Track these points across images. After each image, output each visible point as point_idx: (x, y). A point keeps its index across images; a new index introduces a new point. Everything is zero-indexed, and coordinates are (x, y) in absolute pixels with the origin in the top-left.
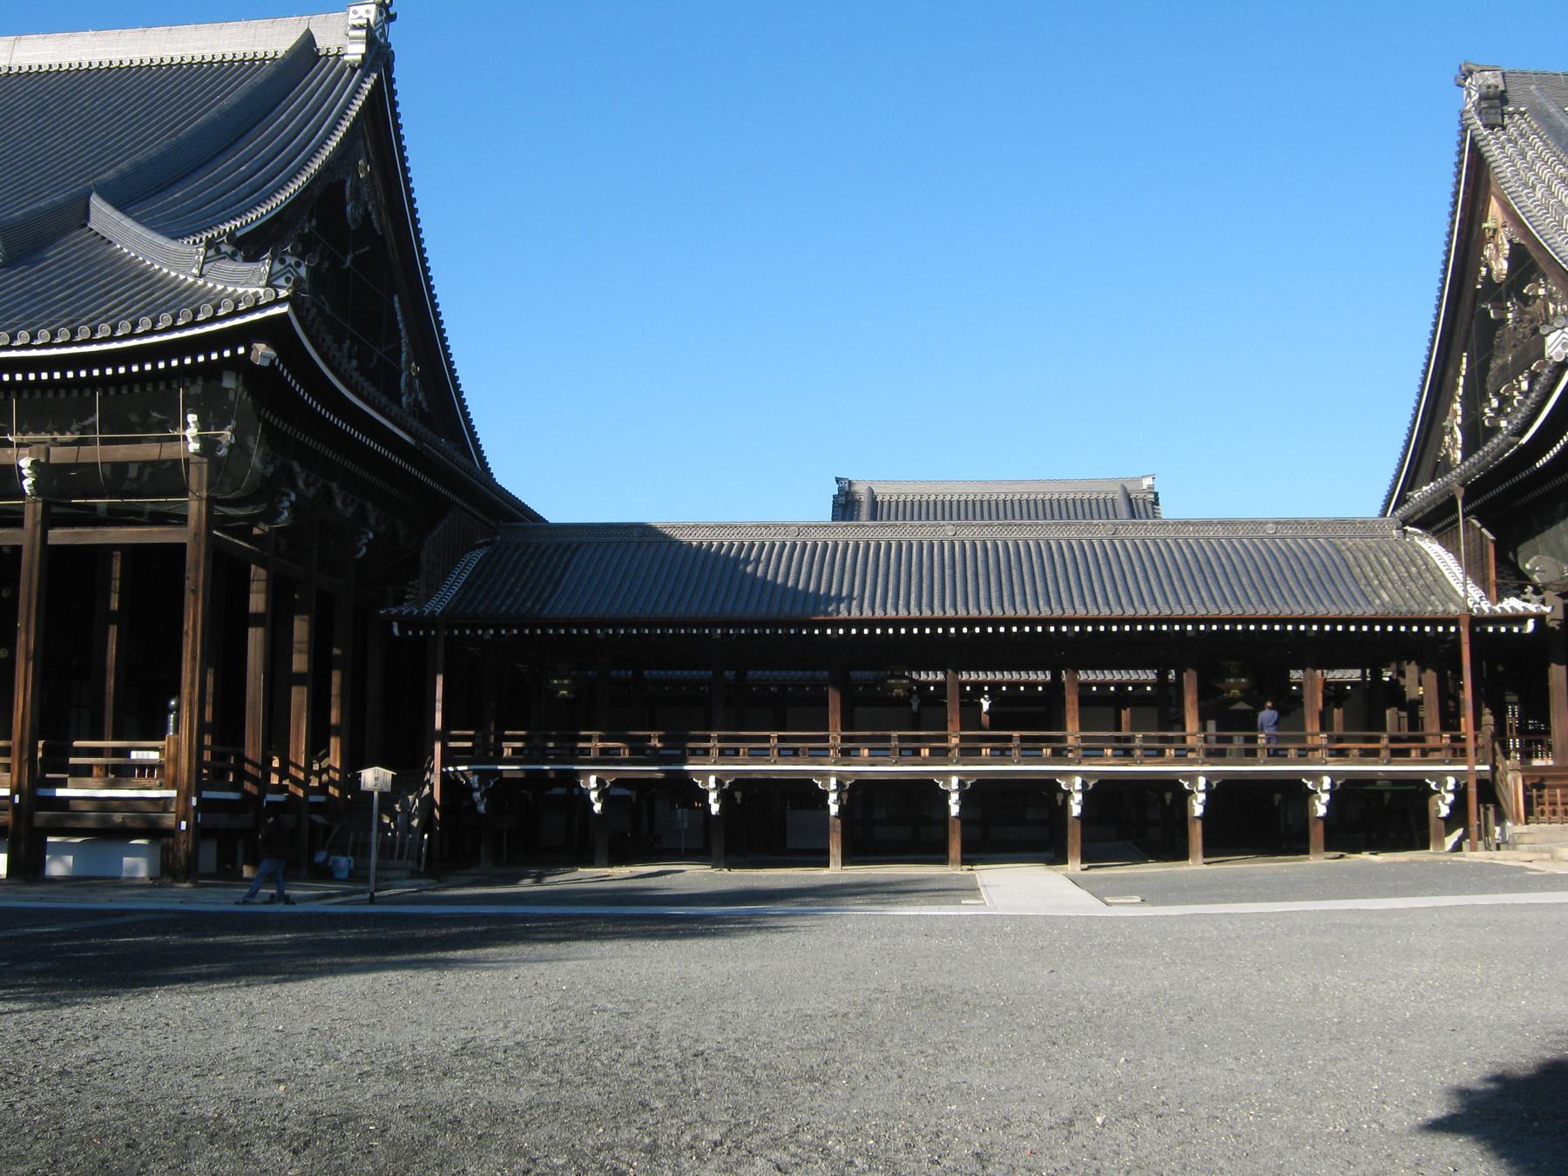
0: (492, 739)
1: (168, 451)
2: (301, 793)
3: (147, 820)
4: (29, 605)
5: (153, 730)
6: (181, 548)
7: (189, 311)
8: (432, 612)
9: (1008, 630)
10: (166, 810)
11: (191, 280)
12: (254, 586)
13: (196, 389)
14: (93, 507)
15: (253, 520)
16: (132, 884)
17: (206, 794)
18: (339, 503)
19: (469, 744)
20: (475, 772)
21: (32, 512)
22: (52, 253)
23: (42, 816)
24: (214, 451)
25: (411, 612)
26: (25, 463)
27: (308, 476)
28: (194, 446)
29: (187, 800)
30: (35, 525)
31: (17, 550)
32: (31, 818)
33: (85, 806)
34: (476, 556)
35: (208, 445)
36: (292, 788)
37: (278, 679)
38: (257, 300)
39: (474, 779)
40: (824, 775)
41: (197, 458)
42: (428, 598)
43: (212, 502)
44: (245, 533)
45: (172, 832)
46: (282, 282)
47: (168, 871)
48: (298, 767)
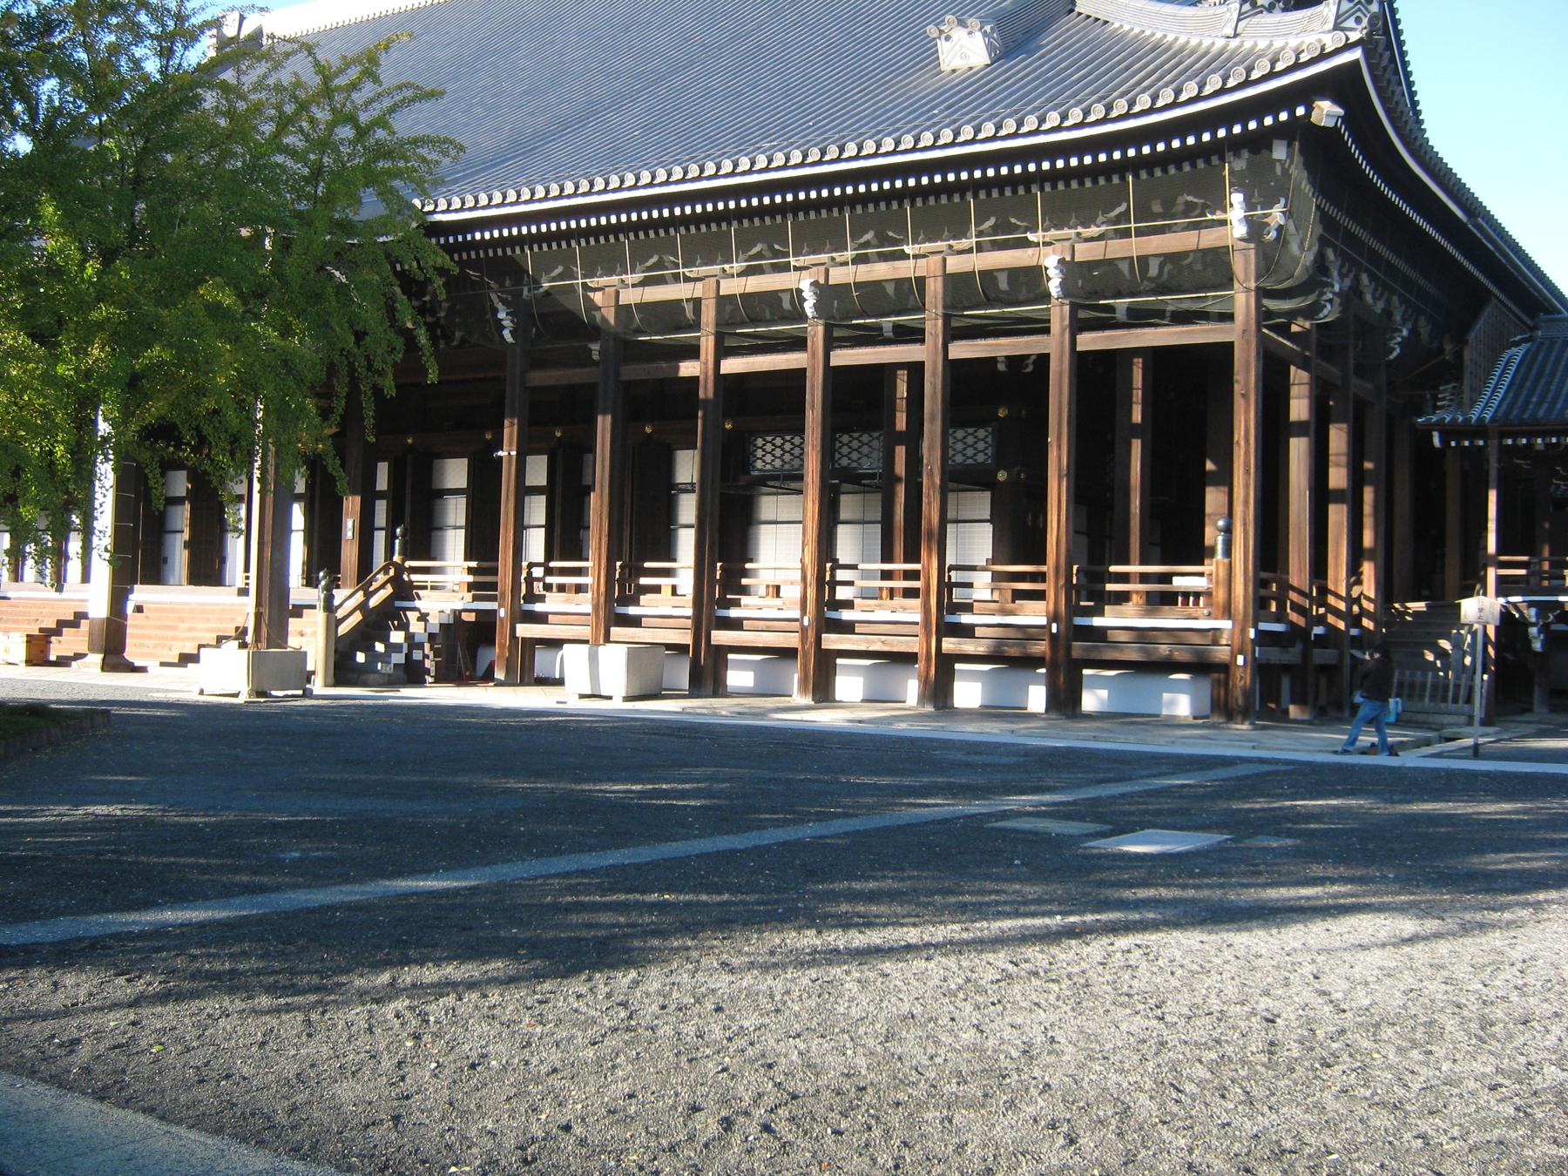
0: (1546, 566)
1: (1209, 238)
2: (1341, 625)
3: (1198, 653)
4: (1060, 415)
5: (1196, 553)
6: (1228, 347)
7: (1241, 70)
8: (1480, 420)
10: (1216, 643)
11: (1220, 43)
12: (1294, 391)
13: (1240, 164)
14: (1111, 309)
15: (1292, 315)
16: (1173, 723)
17: (1263, 626)
18: (1369, 298)
19: (1523, 572)
20: (1531, 604)
21: (1059, 315)
22: (1048, 40)
23: (1078, 648)
24: (1262, 236)
25: (1454, 420)
26: (1050, 261)
27: (1341, 267)
28: (1240, 230)
29: (1244, 632)
30: (1063, 331)
31: (1043, 360)
32: (1069, 648)
33: (1123, 637)
34: (1518, 353)
35: (1256, 228)
36: (1331, 619)
37: (1321, 496)
38: (1323, 48)
39: (1531, 614)
41: (1244, 245)
42: (1473, 403)
43: (1262, 293)
44: (1283, 330)
45: (1225, 668)
46: (1350, 23)
47: (1223, 708)
48: (1338, 596)
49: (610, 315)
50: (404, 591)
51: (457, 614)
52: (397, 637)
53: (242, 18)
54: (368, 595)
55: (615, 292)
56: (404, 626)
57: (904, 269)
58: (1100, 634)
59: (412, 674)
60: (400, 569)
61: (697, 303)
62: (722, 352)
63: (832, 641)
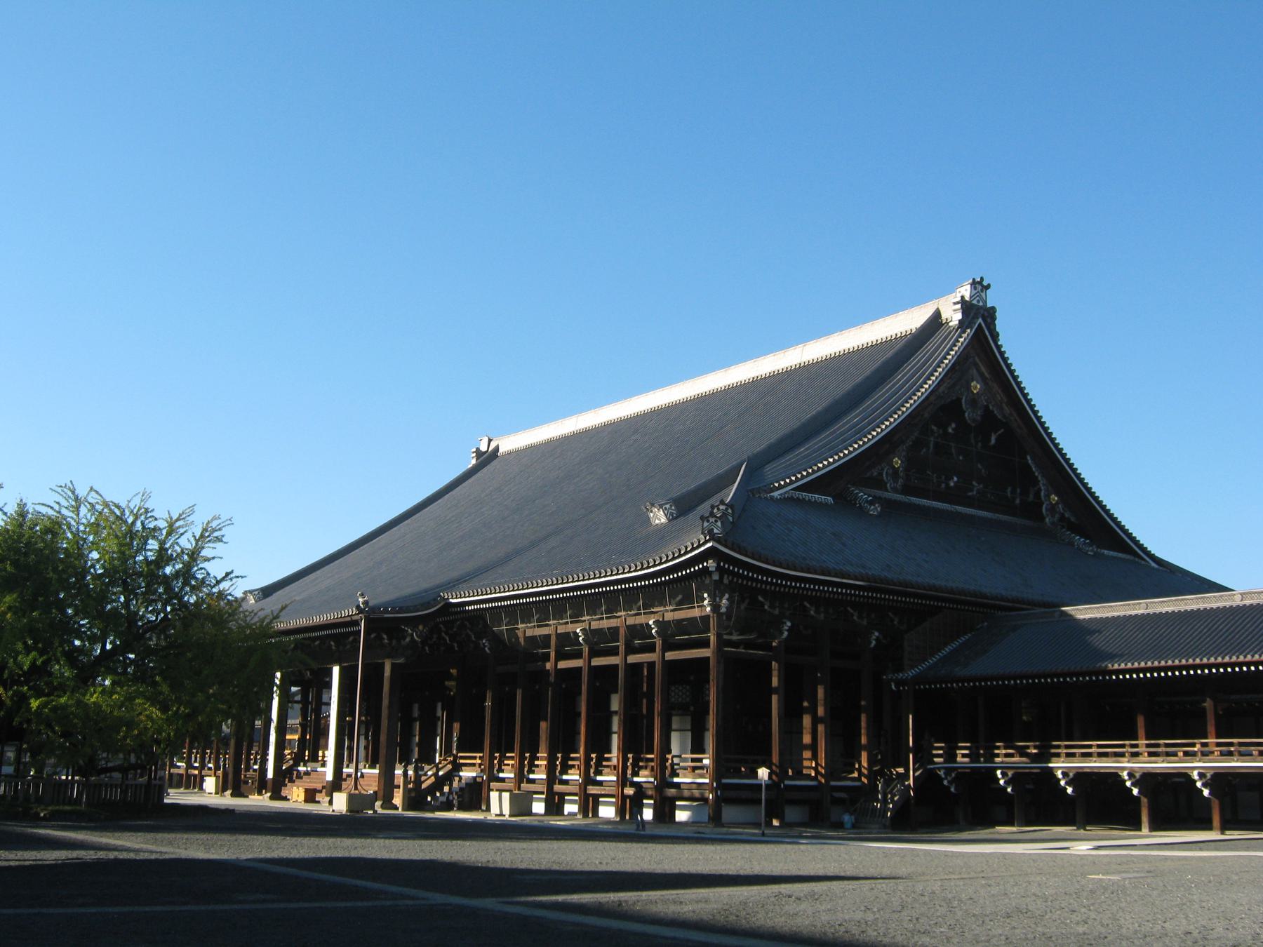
9: (1233, 669)
21: (659, 643)
23: (672, 792)
26: (651, 622)
35: (715, 607)
40: (1123, 769)
49: (522, 640)
50: (457, 767)
51: (475, 778)
52: (446, 789)
53: (490, 441)
54: (438, 770)
55: (528, 630)
56: (451, 785)
57: (613, 623)
58: (678, 785)
59: (448, 806)
60: (456, 757)
61: (548, 637)
62: (558, 659)
63: (593, 790)
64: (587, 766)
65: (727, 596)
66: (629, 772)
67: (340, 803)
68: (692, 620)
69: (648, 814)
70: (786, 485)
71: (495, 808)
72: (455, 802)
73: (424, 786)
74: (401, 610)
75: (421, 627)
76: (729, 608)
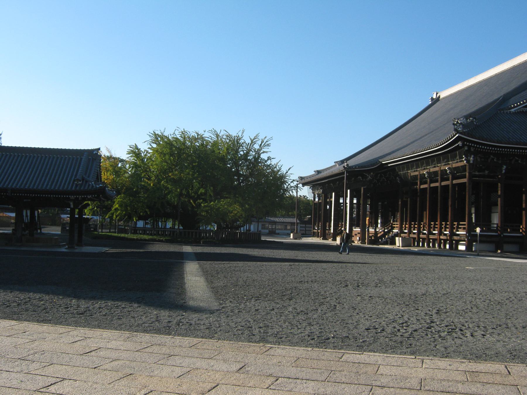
6: (465, 183)
35: (468, 161)
52: (387, 236)
53: (437, 94)
57: (437, 169)
59: (386, 243)
60: (392, 224)
64: (441, 228)
65: (472, 156)
66: (412, 229)
67: (338, 241)
68: (458, 167)
69: (448, 246)
70: (518, 106)
71: (397, 244)
72: (389, 242)
73: (379, 235)
74: (362, 167)
75: (372, 174)
76: (473, 161)
